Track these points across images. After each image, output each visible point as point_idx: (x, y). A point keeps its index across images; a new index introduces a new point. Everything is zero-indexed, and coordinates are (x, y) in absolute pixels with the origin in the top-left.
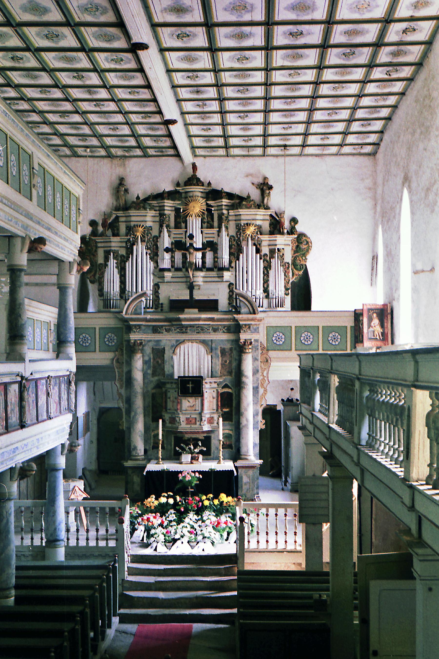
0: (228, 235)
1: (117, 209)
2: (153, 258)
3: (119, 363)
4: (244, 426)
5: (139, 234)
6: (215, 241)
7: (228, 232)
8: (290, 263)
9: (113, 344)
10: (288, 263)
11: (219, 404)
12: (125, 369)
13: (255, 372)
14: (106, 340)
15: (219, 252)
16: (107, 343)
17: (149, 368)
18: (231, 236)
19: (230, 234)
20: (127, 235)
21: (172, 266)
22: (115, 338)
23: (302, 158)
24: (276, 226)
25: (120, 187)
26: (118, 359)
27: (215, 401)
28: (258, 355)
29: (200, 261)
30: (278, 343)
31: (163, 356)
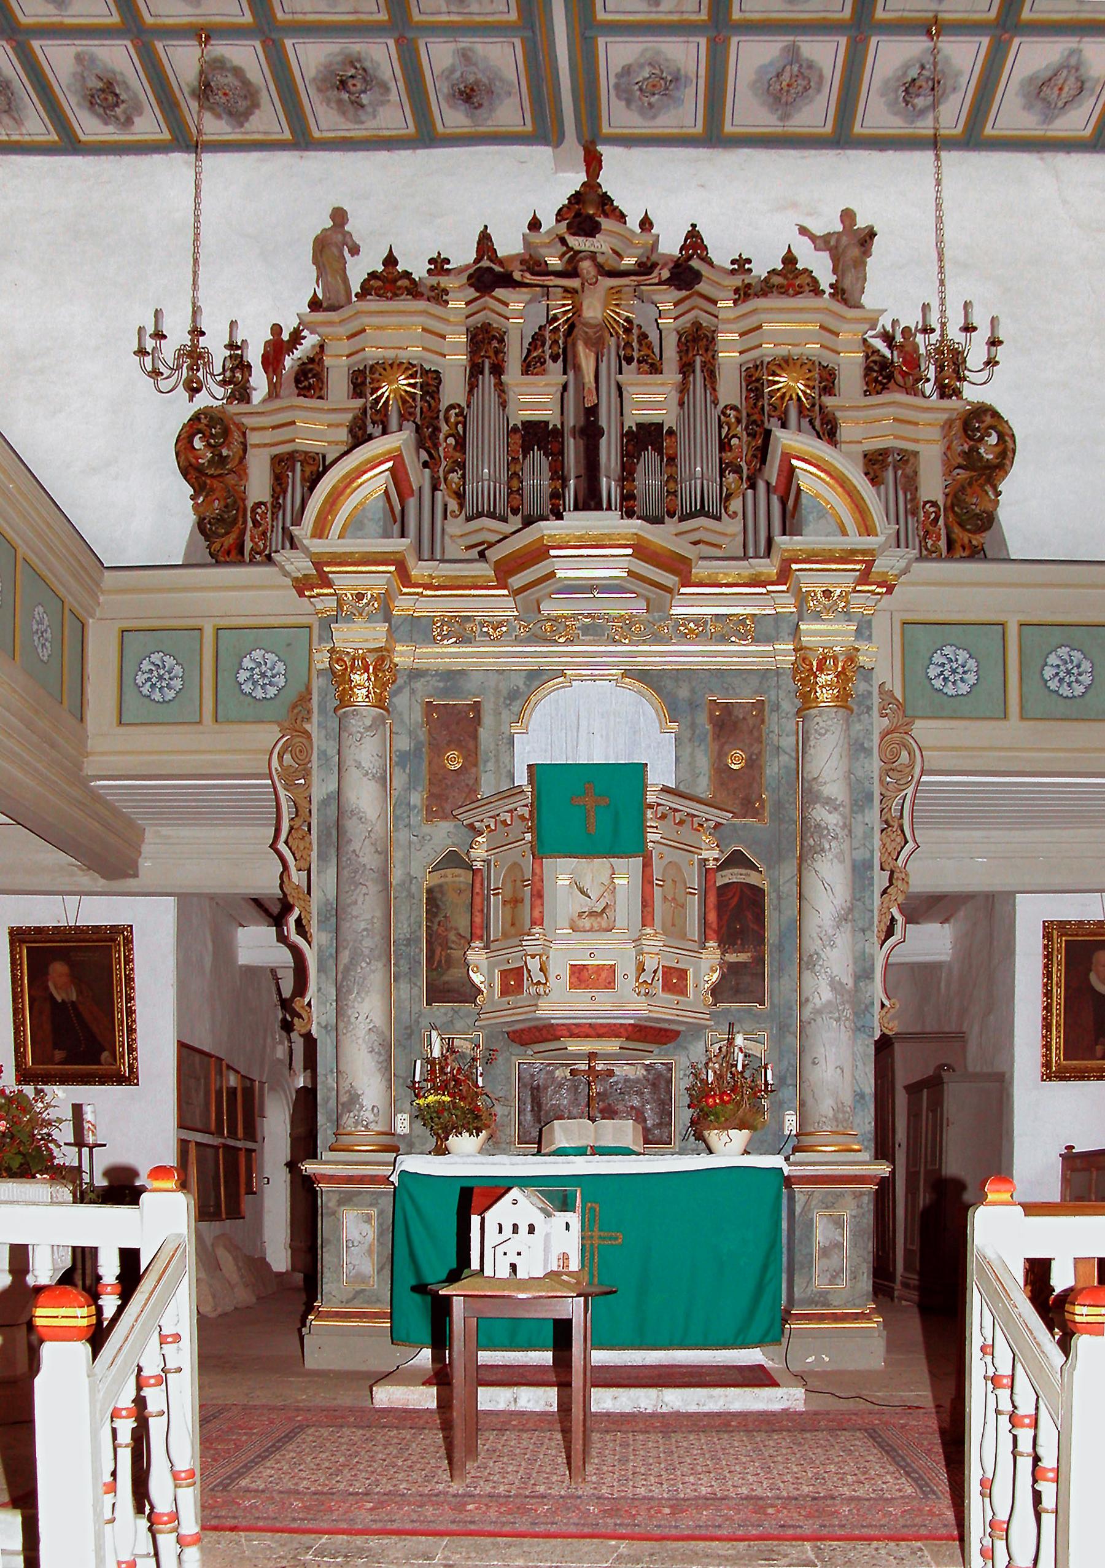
1: (315, 305)
6: (670, 422)
9: (272, 691)
11: (712, 917)
14: (243, 676)
16: (247, 688)
18: (726, 407)
22: (280, 667)
30: (950, 690)
31: (475, 737)
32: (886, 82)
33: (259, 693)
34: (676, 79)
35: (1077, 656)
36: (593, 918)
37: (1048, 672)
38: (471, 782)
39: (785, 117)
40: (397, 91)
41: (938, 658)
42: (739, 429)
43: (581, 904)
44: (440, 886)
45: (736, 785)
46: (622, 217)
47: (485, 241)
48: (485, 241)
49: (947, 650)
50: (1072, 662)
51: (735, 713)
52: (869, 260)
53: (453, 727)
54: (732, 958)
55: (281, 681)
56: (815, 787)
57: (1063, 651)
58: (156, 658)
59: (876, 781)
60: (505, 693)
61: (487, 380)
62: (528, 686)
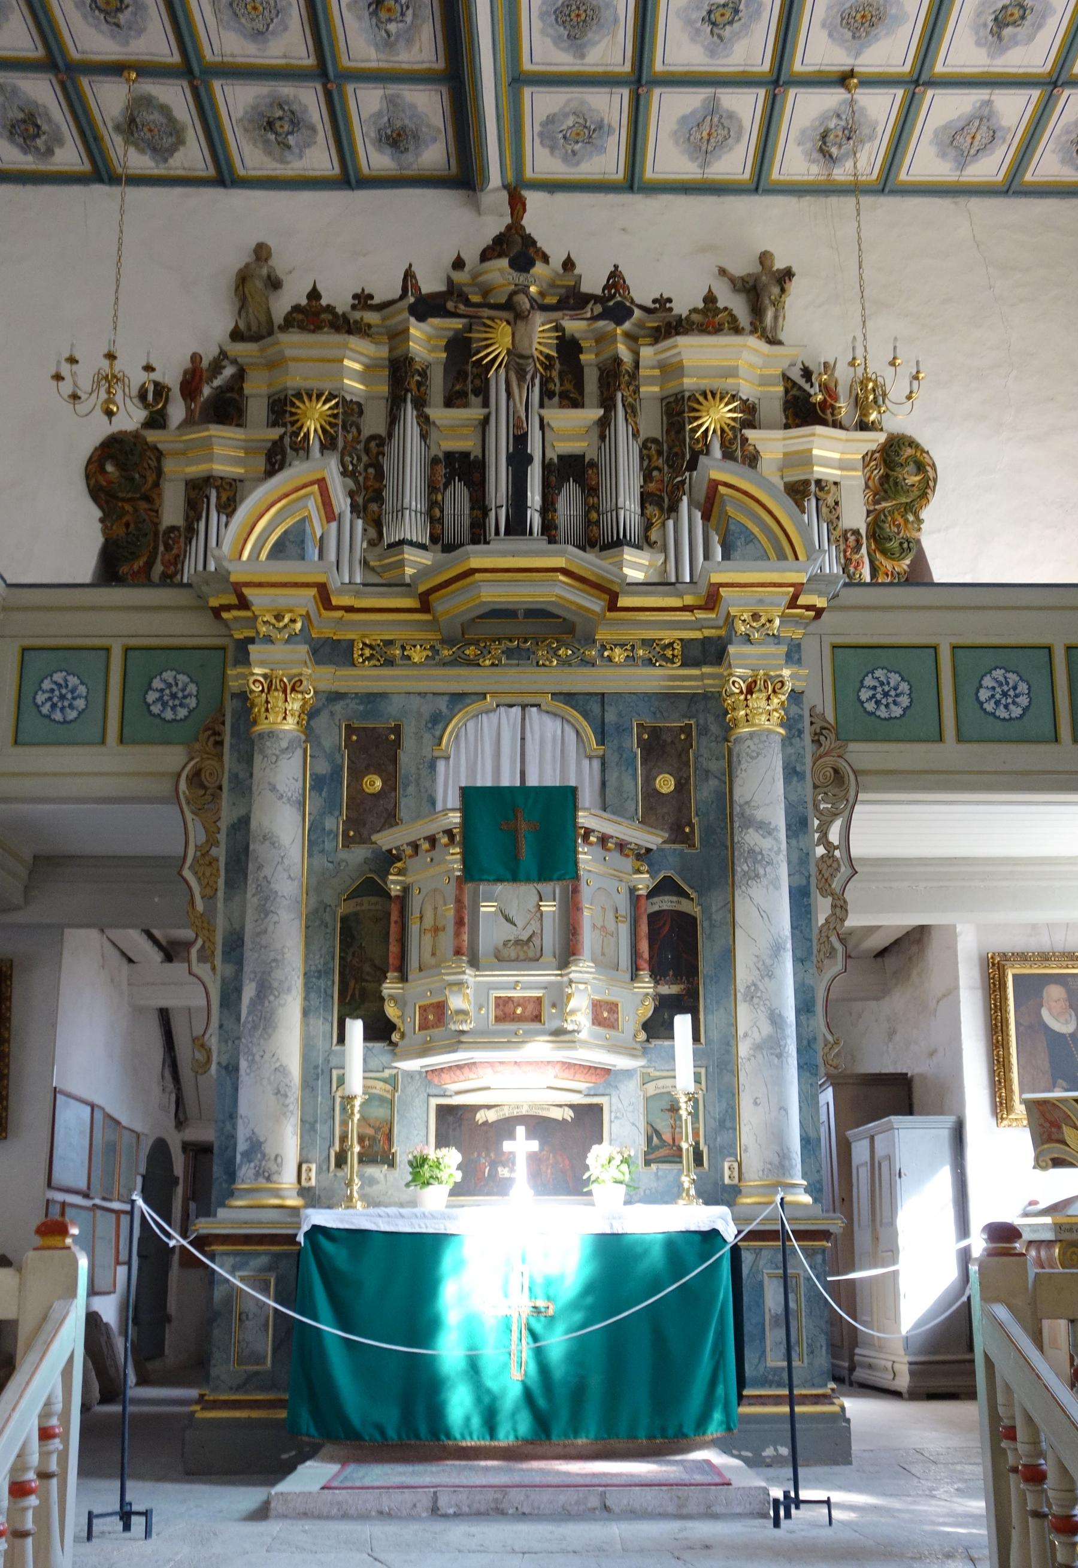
0: (636, 435)
1: (236, 335)
3: (204, 787)
7: (636, 423)
8: (863, 532)
9: (182, 713)
10: (856, 532)
11: (644, 946)
12: (227, 814)
13: (797, 825)
14: (151, 697)
15: (604, 492)
16: (156, 709)
17: (331, 806)
20: (274, 424)
21: (434, 539)
22: (192, 688)
24: (805, 405)
25: (255, 279)
27: (624, 930)
28: (800, 757)
30: (883, 712)
31: (394, 760)
33: (169, 715)
34: (600, 126)
35: (1013, 678)
36: (519, 947)
37: (984, 695)
38: (390, 807)
39: (705, 164)
41: (869, 681)
42: (660, 461)
43: (507, 932)
44: (356, 914)
45: (665, 810)
47: (409, 275)
48: (409, 275)
49: (879, 673)
50: (1007, 683)
51: (664, 737)
54: (665, 990)
55: (192, 702)
56: (748, 812)
57: (998, 674)
58: (58, 677)
59: (810, 805)
62: (452, 710)
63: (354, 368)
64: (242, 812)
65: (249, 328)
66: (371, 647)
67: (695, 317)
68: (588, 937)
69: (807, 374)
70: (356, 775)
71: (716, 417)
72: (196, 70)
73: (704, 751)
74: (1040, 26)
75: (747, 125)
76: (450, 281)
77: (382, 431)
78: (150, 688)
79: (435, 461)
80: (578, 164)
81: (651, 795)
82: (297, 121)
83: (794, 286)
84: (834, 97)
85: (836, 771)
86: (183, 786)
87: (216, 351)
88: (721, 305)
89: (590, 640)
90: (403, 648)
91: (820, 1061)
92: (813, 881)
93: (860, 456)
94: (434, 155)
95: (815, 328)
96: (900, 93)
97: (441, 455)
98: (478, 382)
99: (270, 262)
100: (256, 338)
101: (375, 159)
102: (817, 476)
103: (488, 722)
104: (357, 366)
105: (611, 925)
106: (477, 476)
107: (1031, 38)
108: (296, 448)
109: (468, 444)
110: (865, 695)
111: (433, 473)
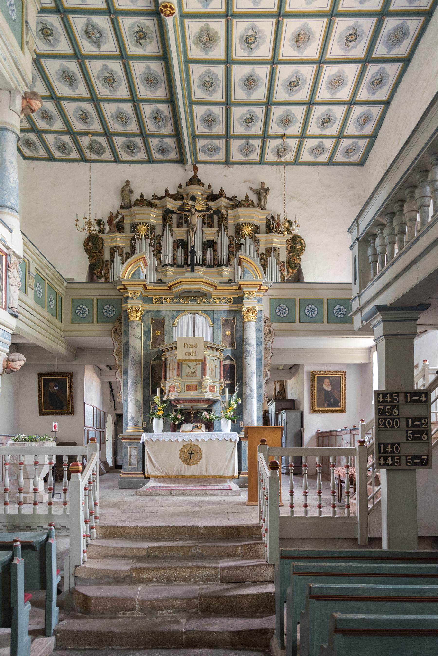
0: (227, 235)
1: (122, 207)
2: (157, 255)
4: (248, 396)
5: (142, 232)
6: (215, 240)
9: (112, 315)
11: (222, 373)
12: (123, 341)
13: (259, 343)
14: (104, 311)
15: (219, 251)
16: (105, 314)
17: (148, 338)
18: (230, 236)
19: (229, 235)
20: (132, 232)
22: (114, 309)
23: (297, 167)
24: (271, 227)
25: (126, 190)
26: (116, 330)
27: (217, 369)
28: (261, 326)
29: (201, 258)
30: (281, 315)
31: (163, 327)
32: (272, 149)
33: (108, 316)
34: (217, 148)
35: (314, 307)
37: (306, 311)
38: (162, 339)
39: (246, 157)
40: (143, 150)
41: (279, 307)
43: (190, 370)
44: (155, 364)
46: (203, 185)
47: (167, 190)
48: (167, 190)
49: (281, 305)
52: (268, 196)
53: (158, 325)
55: (114, 312)
57: (310, 306)
59: (263, 338)
60: (171, 316)
61: (168, 229)
63: (153, 217)
64: (127, 340)
65: (125, 205)
66: (157, 299)
67: (243, 202)
68: (208, 371)
69: (273, 218)
70: (154, 331)
71: (248, 230)
72: (108, 134)
73: (238, 325)
74: (334, 123)
75: (257, 147)
76: (178, 191)
77: (161, 234)
78: (104, 309)
79: (175, 242)
80: (212, 157)
81: (225, 336)
82: (135, 146)
83: (270, 192)
84: (280, 141)
85: (269, 330)
86: (113, 333)
87: (116, 212)
88: (249, 199)
89: (210, 297)
90: (165, 299)
91: (263, 399)
92: (263, 357)
93: (285, 241)
94: (173, 155)
95: (274, 205)
96: (298, 140)
97: (176, 240)
98: (186, 220)
99: (130, 186)
100: (127, 208)
101: (158, 156)
102: (274, 246)
103: (186, 318)
104: (154, 216)
105: (214, 368)
106: (185, 246)
107: (332, 126)
108: (138, 239)
109: (183, 238)
110: (277, 311)
111: (174, 246)
